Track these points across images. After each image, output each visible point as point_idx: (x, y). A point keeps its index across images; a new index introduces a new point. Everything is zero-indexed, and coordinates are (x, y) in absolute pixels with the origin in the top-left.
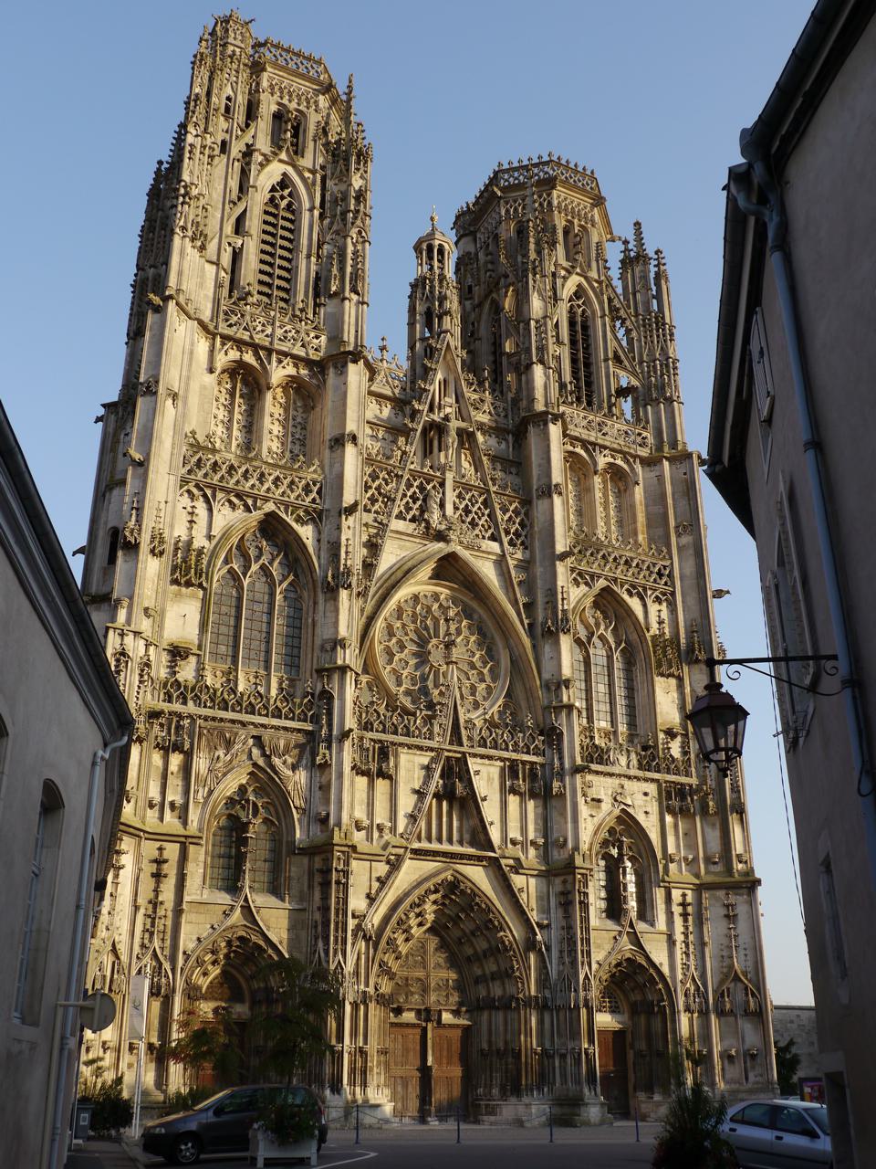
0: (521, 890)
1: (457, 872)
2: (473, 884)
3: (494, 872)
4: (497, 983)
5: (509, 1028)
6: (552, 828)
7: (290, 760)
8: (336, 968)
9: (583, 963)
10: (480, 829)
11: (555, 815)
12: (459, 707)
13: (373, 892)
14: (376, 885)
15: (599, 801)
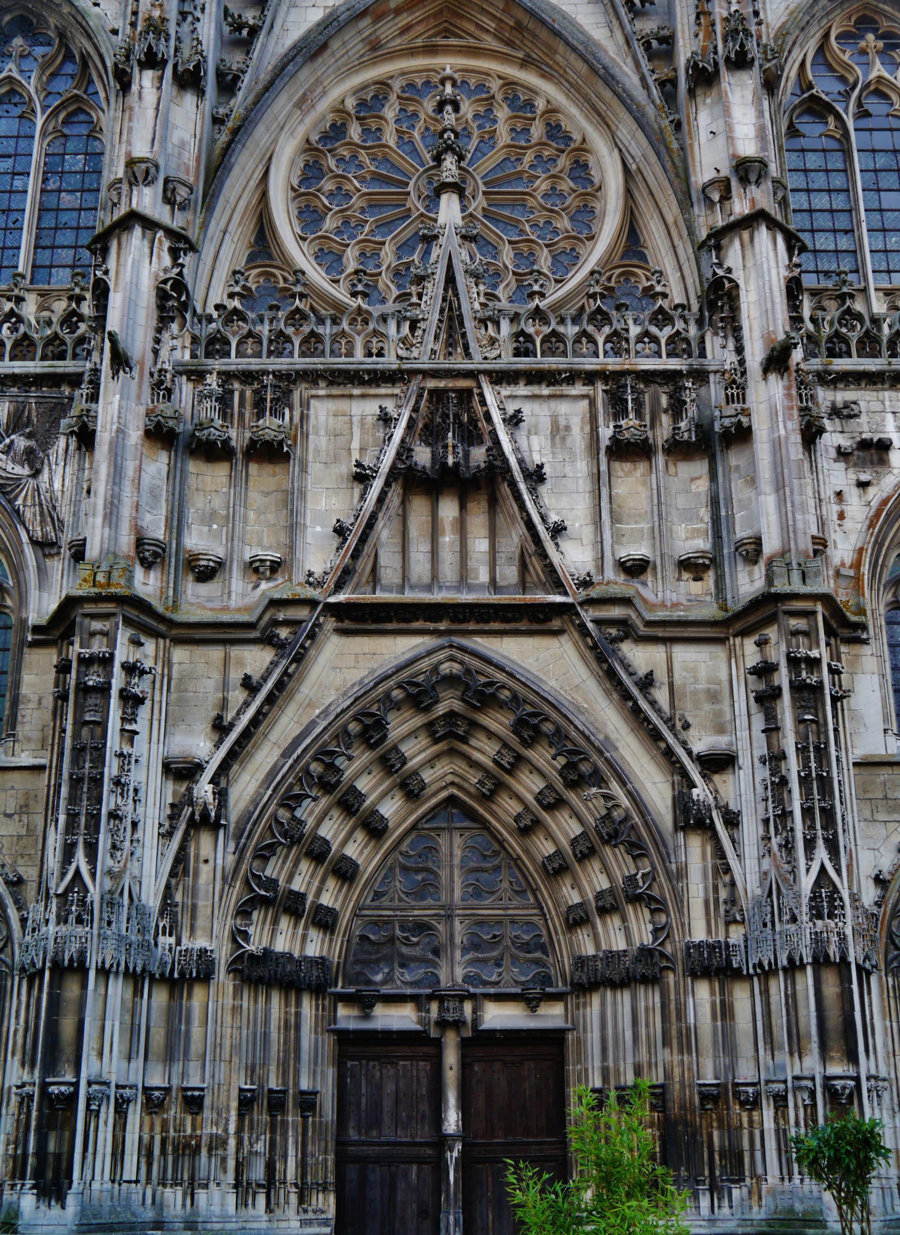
0: (647, 683)
1: (463, 649)
2: (511, 675)
3: (575, 644)
4: (615, 922)
5: (643, 1031)
6: (731, 518)
7: (21, 443)
8: (68, 889)
9: (810, 845)
10: (531, 548)
11: (739, 489)
12: (460, 278)
13: (229, 716)
14: (238, 696)
15: (884, 446)
